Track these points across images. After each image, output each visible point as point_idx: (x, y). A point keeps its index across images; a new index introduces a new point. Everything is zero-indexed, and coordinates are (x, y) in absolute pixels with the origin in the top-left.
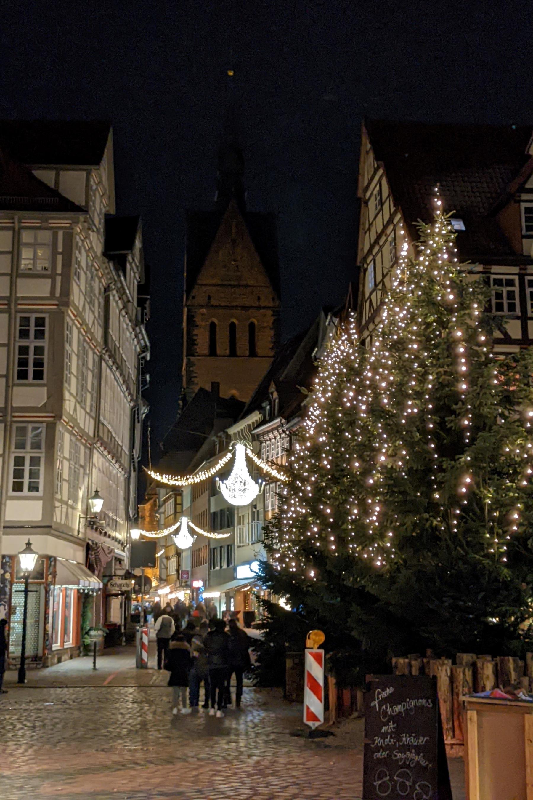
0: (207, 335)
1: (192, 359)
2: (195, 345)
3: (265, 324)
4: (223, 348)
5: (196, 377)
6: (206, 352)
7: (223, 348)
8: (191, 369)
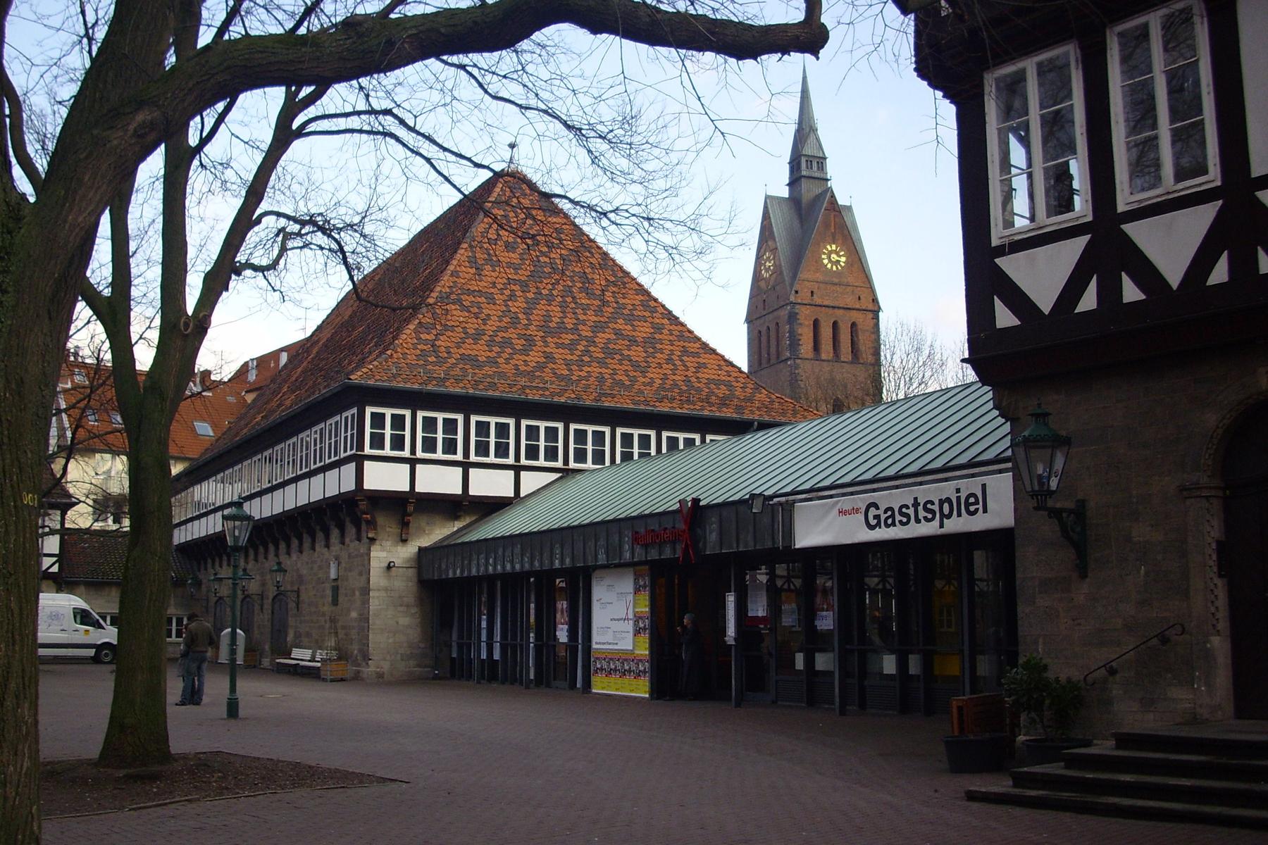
6: (811, 355)
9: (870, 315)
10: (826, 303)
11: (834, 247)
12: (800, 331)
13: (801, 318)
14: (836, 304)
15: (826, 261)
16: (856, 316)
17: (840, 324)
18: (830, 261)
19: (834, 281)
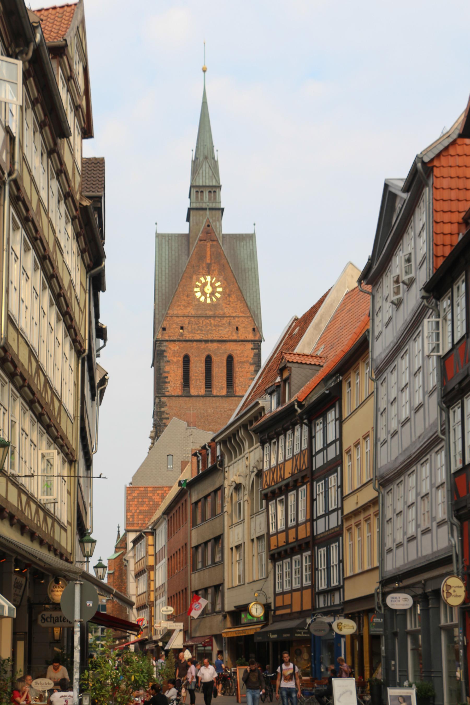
0: (180, 372)
1: (163, 399)
2: (166, 382)
3: (244, 359)
5: (168, 418)
6: (179, 391)
8: (162, 409)
9: (250, 346)
10: (198, 337)
11: (209, 278)
12: (167, 368)
13: (169, 355)
14: (210, 337)
15: (198, 295)
16: (231, 348)
17: (214, 358)
18: (204, 293)
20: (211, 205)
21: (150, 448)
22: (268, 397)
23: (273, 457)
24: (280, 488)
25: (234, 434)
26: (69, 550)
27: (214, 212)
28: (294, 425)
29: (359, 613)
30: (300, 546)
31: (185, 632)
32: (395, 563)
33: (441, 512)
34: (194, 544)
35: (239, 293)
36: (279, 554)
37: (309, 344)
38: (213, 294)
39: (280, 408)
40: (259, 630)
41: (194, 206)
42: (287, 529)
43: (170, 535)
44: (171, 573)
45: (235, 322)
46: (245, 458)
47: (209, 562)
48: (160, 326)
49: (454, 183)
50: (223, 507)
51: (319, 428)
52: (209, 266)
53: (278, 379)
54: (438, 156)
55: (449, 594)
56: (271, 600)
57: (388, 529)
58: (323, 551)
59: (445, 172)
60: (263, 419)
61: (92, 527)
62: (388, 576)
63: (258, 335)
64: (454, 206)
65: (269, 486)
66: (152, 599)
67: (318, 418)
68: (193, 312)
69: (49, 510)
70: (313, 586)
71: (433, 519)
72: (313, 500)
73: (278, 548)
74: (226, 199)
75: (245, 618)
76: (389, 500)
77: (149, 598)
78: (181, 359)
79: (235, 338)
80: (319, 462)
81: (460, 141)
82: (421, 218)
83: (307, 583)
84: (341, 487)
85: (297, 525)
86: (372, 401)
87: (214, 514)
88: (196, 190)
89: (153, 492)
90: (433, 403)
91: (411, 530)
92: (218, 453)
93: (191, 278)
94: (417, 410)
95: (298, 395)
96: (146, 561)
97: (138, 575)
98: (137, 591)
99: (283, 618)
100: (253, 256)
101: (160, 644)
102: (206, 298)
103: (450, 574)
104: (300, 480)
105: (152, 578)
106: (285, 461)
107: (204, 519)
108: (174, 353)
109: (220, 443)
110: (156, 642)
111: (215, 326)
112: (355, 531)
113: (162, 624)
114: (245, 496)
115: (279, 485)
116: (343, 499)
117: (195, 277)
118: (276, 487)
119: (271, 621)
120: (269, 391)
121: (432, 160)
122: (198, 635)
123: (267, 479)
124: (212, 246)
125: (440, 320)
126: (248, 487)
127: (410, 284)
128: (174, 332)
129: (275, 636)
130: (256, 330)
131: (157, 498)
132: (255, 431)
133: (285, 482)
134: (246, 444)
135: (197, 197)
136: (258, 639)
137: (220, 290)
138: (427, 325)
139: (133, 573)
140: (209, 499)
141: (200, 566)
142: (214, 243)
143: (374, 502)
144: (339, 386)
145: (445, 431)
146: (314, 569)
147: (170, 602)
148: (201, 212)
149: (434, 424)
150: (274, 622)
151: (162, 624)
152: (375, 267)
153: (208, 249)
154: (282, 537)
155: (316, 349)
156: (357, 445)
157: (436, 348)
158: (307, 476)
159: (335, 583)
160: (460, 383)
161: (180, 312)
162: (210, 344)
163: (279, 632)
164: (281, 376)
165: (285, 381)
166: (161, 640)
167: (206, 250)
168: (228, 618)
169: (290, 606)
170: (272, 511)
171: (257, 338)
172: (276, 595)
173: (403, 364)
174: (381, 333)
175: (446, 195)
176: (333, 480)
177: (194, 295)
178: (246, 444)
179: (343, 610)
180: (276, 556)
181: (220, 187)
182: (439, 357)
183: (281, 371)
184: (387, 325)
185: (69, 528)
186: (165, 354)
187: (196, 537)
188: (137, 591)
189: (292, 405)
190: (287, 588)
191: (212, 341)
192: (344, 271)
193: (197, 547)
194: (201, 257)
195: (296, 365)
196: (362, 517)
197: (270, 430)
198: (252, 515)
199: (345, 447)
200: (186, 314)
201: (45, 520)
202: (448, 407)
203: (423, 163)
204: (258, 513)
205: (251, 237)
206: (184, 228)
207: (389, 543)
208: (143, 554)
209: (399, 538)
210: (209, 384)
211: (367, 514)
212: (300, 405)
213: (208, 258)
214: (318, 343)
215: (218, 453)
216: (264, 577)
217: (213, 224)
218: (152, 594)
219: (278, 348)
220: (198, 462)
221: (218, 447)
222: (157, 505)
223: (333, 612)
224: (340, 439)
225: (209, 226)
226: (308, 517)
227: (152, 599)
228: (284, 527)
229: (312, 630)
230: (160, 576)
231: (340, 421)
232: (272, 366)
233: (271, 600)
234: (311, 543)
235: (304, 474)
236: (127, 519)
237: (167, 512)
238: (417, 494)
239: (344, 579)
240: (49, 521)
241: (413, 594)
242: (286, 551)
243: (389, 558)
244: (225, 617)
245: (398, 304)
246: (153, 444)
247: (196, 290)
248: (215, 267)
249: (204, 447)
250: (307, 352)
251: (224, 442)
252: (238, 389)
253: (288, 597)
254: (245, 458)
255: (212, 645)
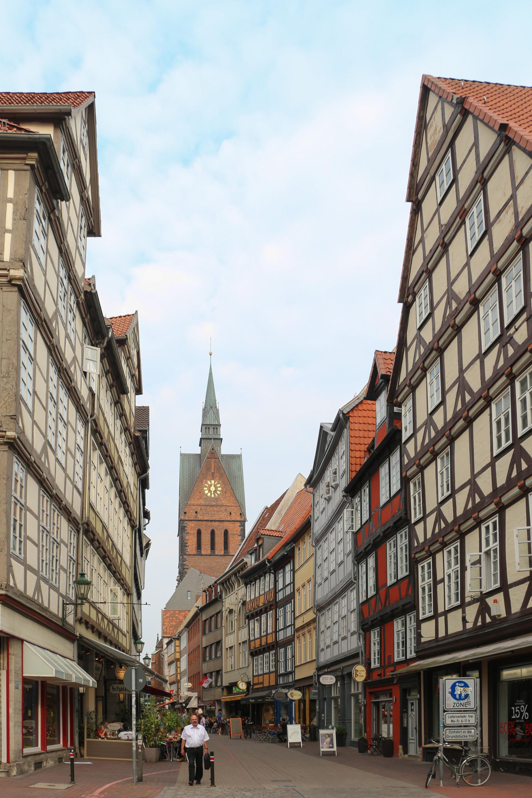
0: (195, 539)
1: (185, 557)
4: (206, 549)
6: (194, 552)
7: (206, 549)
8: (184, 563)
9: (239, 524)
10: (206, 518)
11: (213, 482)
12: (187, 538)
13: (188, 529)
14: (214, 519)
15: (206, 492)
16: (227, 525)
17: (216, 531)
18: (210, 491)
19: (213, 504)
20: (214, 437)
21: (177, 587)
22: (249, 556)
23: (253, 593)
24: (256, 612)
25: (229, 579)
26: (128, 648)
27: (216, 441)
28: (265, 573)
29: (304, 687)
30: (269, 647)
31: (199, 698)
32: (326, 657)
33: (353, 626)
34: (204, 646)
35: (232, 491)
36: (256, 652)
37: (274, 523)
38: (215, 491)
39: (257, 563)
40: (243, 697)
41: (204, 437)
42: (261, 637)
43: (189, 640)
44: (190, 663)
45: (229, 509)
46: (235, 594)
47: (213, 657)
48: (183, 511)
49: (362, 427)
50: (221, 624)
51: (281, 575)
52: (213, 474)
53: (256, 545)
54: (352, 410)
55: (357, 675)
56: (251, 680)
57: (322, 637)
58: (282, 650)
59: (356, 420)
60: (246, 570)
61: (141, 635)
62: (321, 665)
63: (243, 518)
64: (362, 441)
65: (250, 611)
66: (179, 678)
67: (280, 569)
68: (203, 503)
69: (115, 624)
70: (276, 671)
71: (349, 631)
72: (276, 620)
73: (255, 648)
74: (223, 433)
75: (235, 690)
76: (322, 619)
77: (177, 678)
78: (196, 532)
79: (229, 519)
80: (280, 596)
81: (365, 402)
82: (342, 447)
83: (272, 669)
84: (294, 611)
85: (267, 635)
86: (312, 560)
87: (216, 628)
88: (205, 427)
89: (179, 614)
90: (349, 561)
91: (335, 638)
92: (219, 591)
93: (202, 481)
94: (340, 565)
95: (268, 555)
96: (175, 655)
97: (170, 664)
98: (169, 673)
99: (258, 690)
100: (240, 468)
101: (184, 705)
102: (211, 494)
103: (358, 663)
104: (269, 607)
105: (178, 666)
106: (260, 595)
107: (210, 631)
108: (192, 528)
109: (220, 584)
110: (181, 704)
111: (217, 511)
112: (302, 638)
113: (185, 693)
114: (235, 616)
115: (256, 610)
116: (295, 619)
117: (204, 481)
118: (254, 611)
119: (251, 692)
120: (250, 552)
121: (349, 412)
122: (206, 700)
123: (249, 607)
124: (215, 462)
125: (354, 510)
126: (237, 612)
127: (336, 487)
128: (191, 515)
129: (253, 701)
130: (242, 514)
131: (181, 618)
132: (242, 577)
133: (259, 609)
134: (236, 585)
135: (206, 432)
136: (243, 702)
137: (220, 489)
138: (346, 513)
139: (167, 663)
140: (213, 619)
141: (208, 659)
142: (217, 460)
143: (314, 621)
144: (293, 550)
145: (356, 578)
146: (277, 661)
147: (189, 680)
148: (208, 441)
149: (350, 574)
150: (252, 692)
151: (185, 693)
152: (315, 477)
153: (213, 464)
154: (258, 642)
155: (279, 527)
156: (303, 586)
157: (352, 527)
158: (273, 605)
159: (289, 670)
160: (365, 549)
161: (195, 502)
162: (213, 523)
163: (256, 698)
164: (258, 543)
165: (260, 546)
166: (184, 703)
167: (211, 464)
168: (225, 689)
169: (262, 683)
170: (251, 626)
171: (242, 520)
172: (254, 676)
173: (331, 536)
174: (318, 517)
175: (357, 434)
176: (289, 607)
177: (204, 492)
178: (236, 585)
179: (294, 685)
180: (254, 654)
181: (220, 425)
182: (353, 532)
183: (257, 540)
184: (322, 512)
185: (128, 635)
186: (186, 528)
187: (205, 641)
188: (169, 673)
189: (264, 561)
190: (260, 672)
191: (215, 521)
192: (296, 479)
193: (206, 648)
194: (208, 469)
195: (267, 537)
196: (306, 630)
197: (250, 577)
198: (239, 629)
199: (296, 588)
200: (199, 504)
201: (113, 630)
202: (358, 563)
203: (343, 414)
204: (243, 627)
205: (239, 457)
206: (198, 450)
207: (322, 646)
208: (173, 651)
209: (328, 642)
210: (213, 547)
211: (309, 628)
212: (269, 561)
213: (213, 469)
214: (280, 523)
215: (219, 591)
216: (247, 666)
217: (216, 448)
218: (178, 675)
219: (255, 526)
220: (206, 596)
221: (219, 587)
222: (181, 622)
223: (288, 686)
224: (293, 582)
225: (213, 449)
226: (274, 630)
227: (179, 678)
228: (259, 636)
229: (275, 697)
230: (184, 665)
231: (294, 571)
232: (252, 537)
233: (251, 680)
234: (275, 646)
235: (271, 603)
236: (163, 630)
237: (187, 626)
238: (339, 616)
239: (295, 667)
240: (116, 630)
241: (336, 675)
242: (260, 650)
243: (322, 655)
244: (223, 689)
245: (328, 500)
246: (178, 584)
247: (205, 489)
248: (217, 475)
249: (210, 587)
250: (273, 528)
251: (222, 584)
252: (231, 551)
253: (261, 678)
254: (235, 594)
255: (215, 706)
